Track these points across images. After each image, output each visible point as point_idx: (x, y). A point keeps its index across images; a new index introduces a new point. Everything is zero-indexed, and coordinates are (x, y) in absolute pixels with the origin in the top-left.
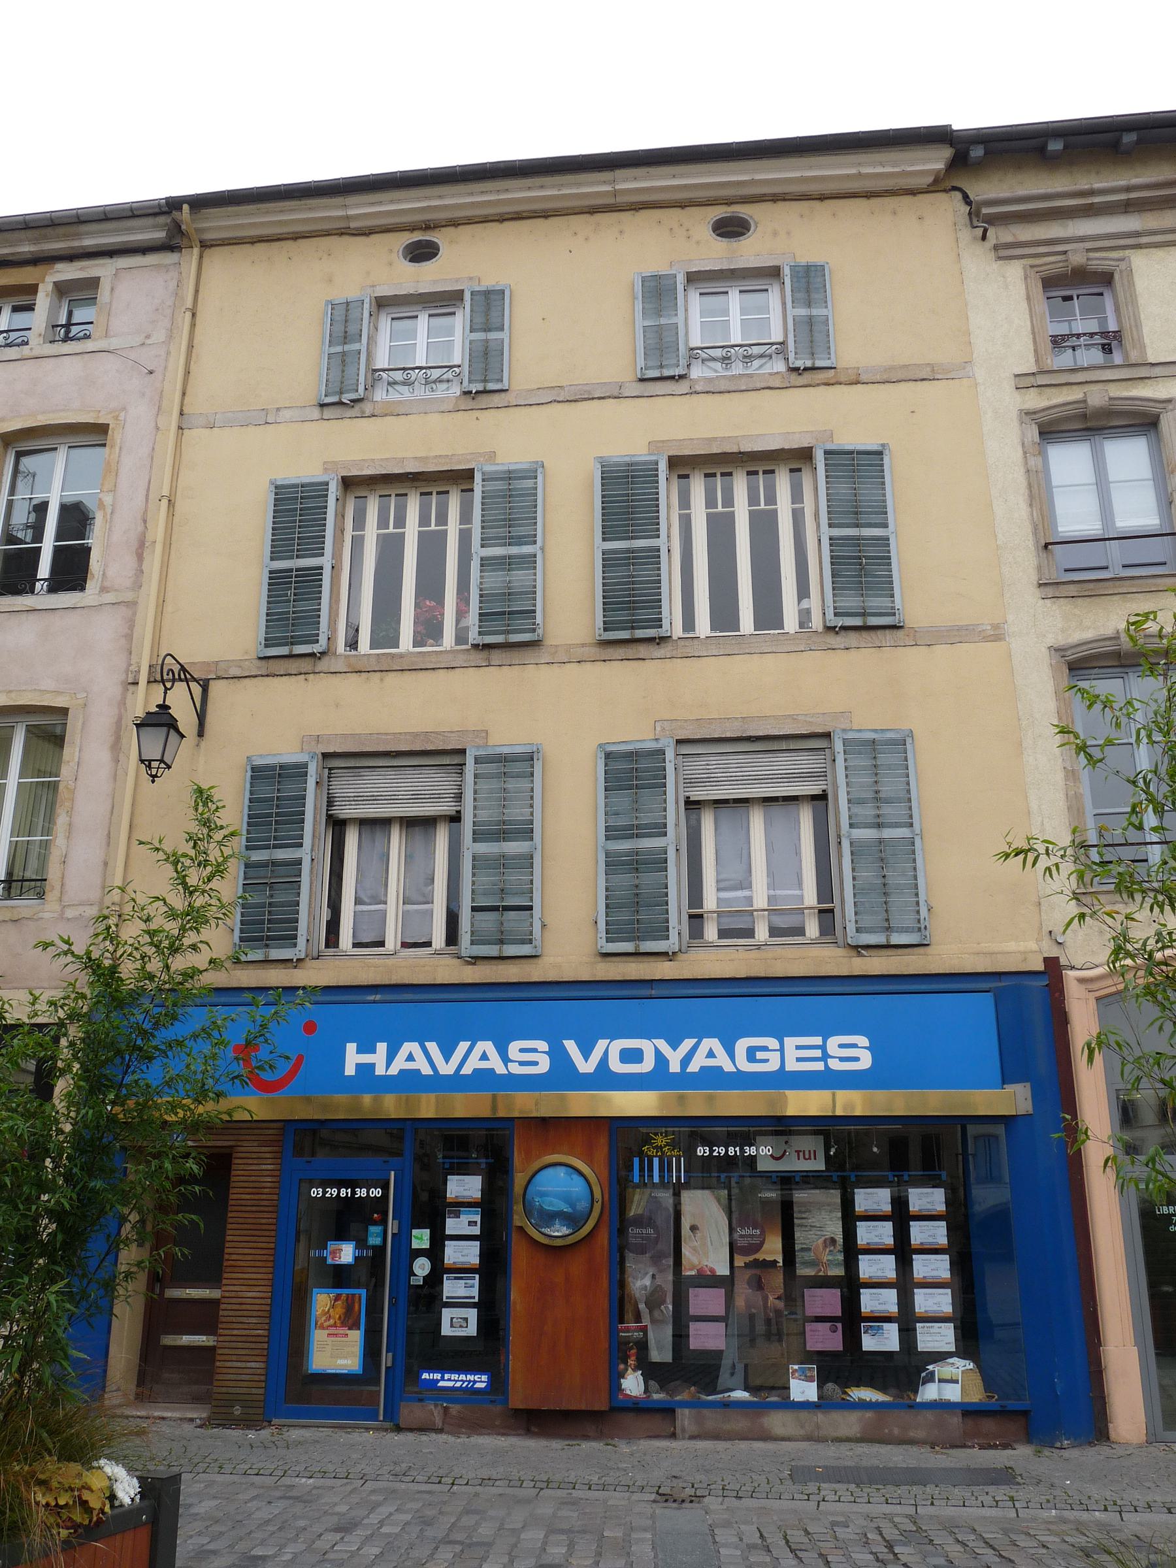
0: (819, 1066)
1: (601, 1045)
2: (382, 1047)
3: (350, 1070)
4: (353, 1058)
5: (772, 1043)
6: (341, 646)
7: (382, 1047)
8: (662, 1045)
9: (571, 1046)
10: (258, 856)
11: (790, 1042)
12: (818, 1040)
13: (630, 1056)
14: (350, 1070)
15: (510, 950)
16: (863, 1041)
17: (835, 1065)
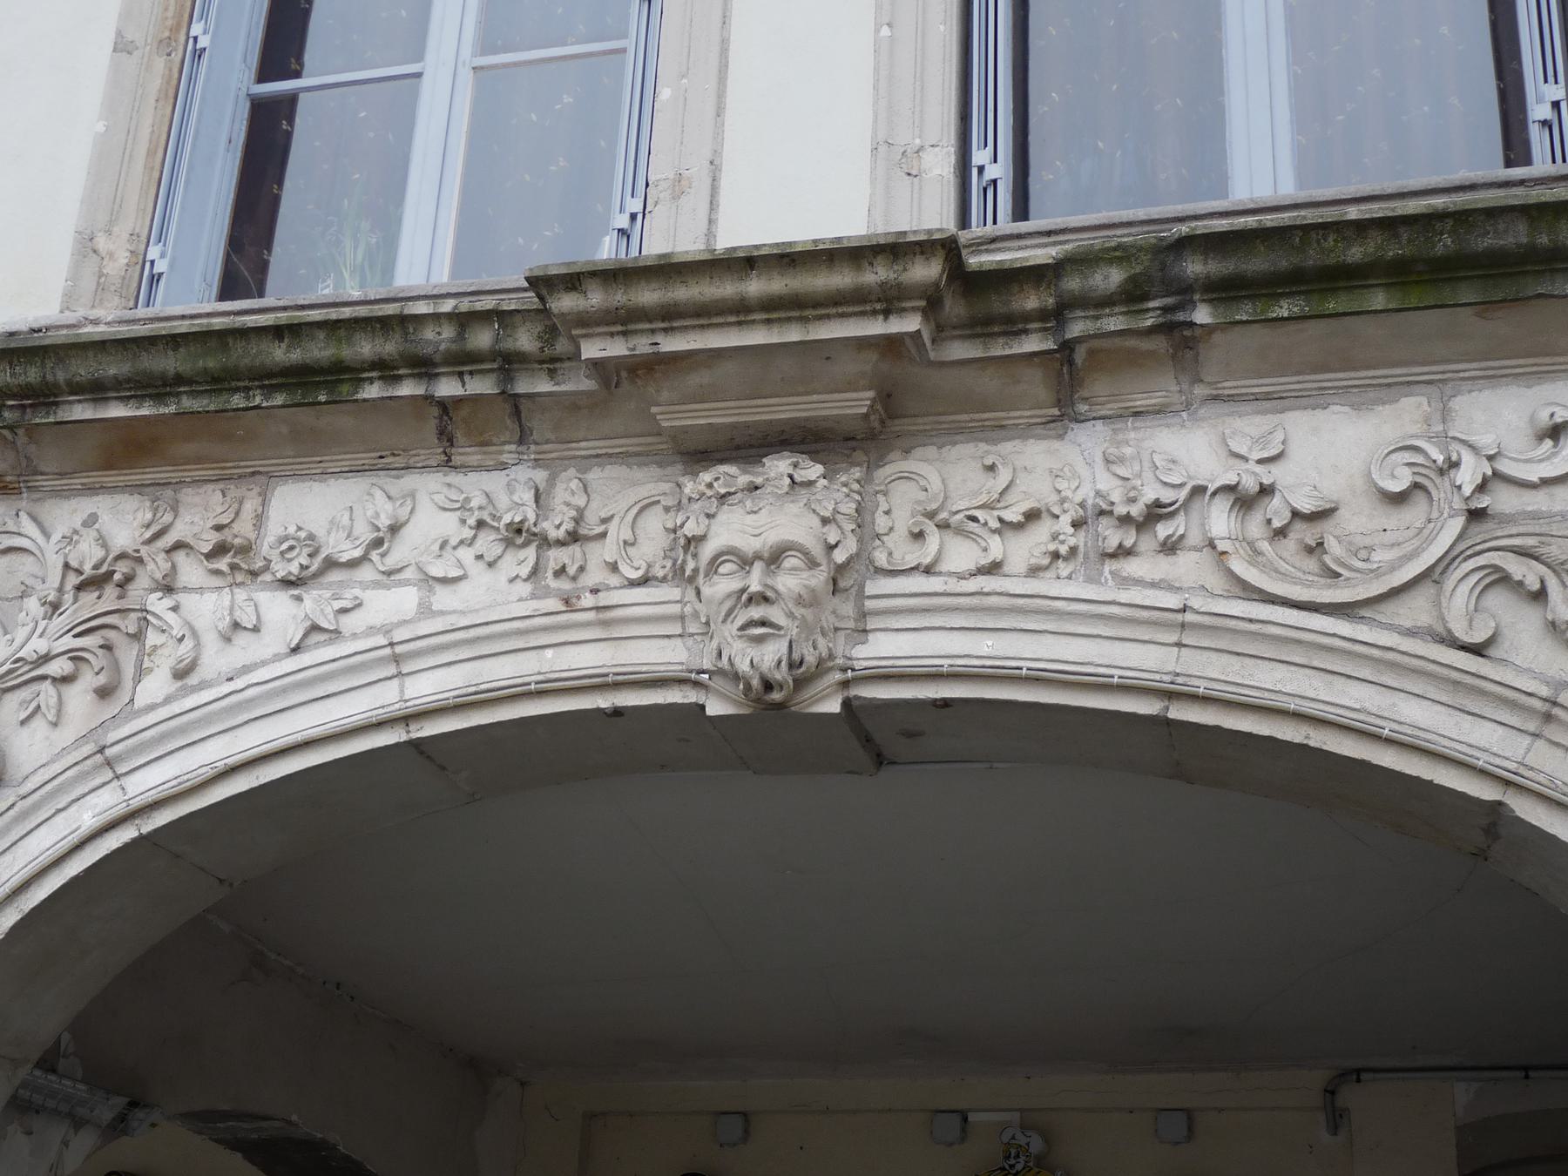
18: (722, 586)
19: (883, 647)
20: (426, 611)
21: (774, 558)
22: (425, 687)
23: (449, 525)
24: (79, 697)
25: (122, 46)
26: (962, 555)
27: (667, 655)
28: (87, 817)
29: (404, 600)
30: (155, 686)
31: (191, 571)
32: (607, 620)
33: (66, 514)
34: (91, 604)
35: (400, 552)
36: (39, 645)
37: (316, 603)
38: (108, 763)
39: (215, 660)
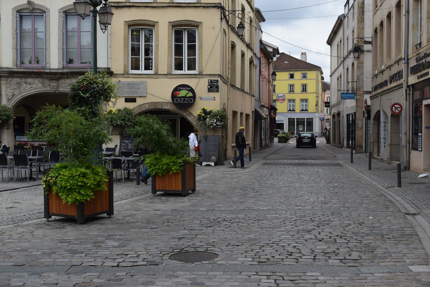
18: (52, 87)
19: (60, 89)
20: (37, 87)
21: (54, 86)
22: (37, 90)
23: (37, 82)
24: (18, 90)
25: (13, 48)
26: (63, 85)
27: (49, 89)
28: (20, 96)
29: (35, 86)
30: (22, 90)
31: (23, 83)
32: (46, 88)
33: (15, 79)
34: (18, 85)
35: (35, 83)
36: (15, 87)
37: (31, 86)
38: (20, 94)
39: (26, 88)
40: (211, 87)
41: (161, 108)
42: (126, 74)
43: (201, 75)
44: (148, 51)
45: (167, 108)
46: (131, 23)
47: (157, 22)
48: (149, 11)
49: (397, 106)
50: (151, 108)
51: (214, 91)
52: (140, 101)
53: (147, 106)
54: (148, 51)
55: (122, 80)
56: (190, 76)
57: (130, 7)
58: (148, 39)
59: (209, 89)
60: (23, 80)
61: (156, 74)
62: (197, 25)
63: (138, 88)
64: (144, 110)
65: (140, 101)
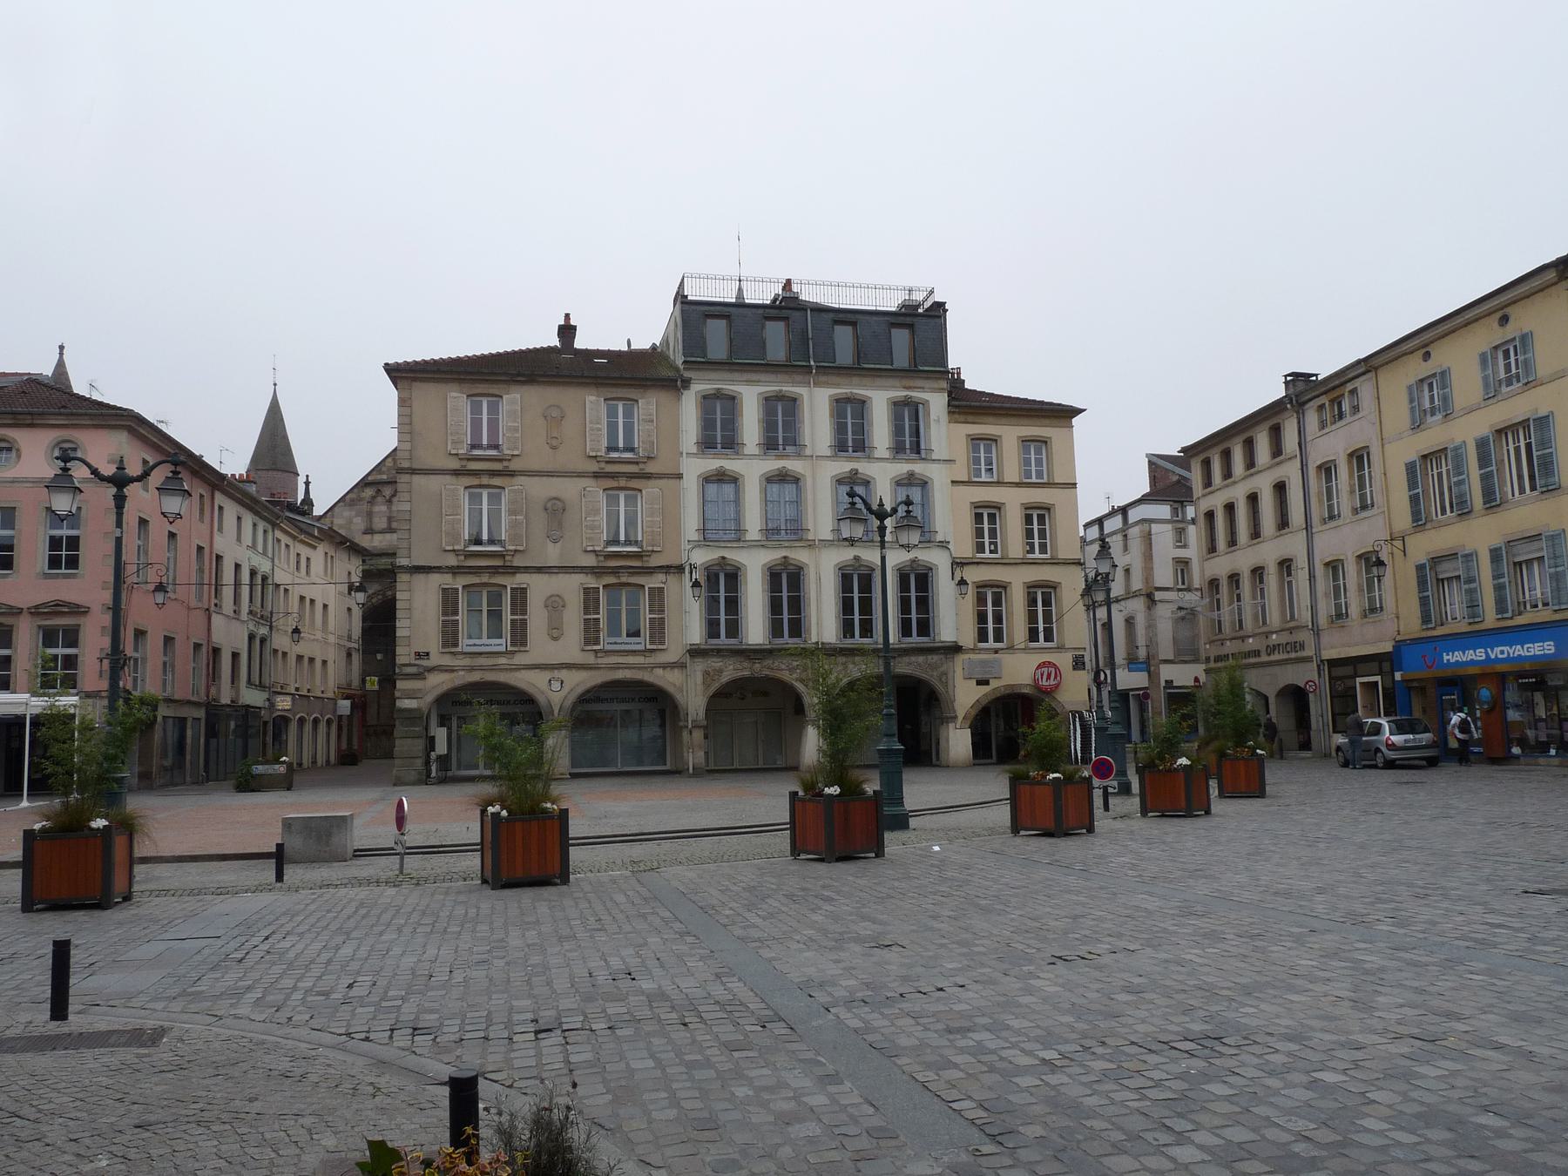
0: (1542, 652)
1: (1495, 649)
2: (1451, 654)
3: (1445, 661)
4: (1446, 657)
5: (1531, 645)
6: (1434, 518)
7: (1451, 654)
8: (1508, 648)
9: (1489, 649)
10: (1421, 595)
11: (1536, 644)
12: (1541, 644)
13: (1502, 652)
14: (1445, 661)
15: (1476, 620)
16: (1552, 643)
17: (1546, 652)
19: (896, 670)
40: (1076, 664)
41: (1019, 691)
42: (973, 650)
43: (1061, 648)
44: (998, 619)
45: (1026, 691)
46: (981, 584)
47: (1010, 583)
48: (999, 569)
49: (1310, 683)
50: (1007, 692)
51: (1080, 669)
52: (994, 684)
53: (1002, 689)
54: (998, 619)
55: (972, 656)
56: (1051, 651)
57: (978, 563)
58: (997, 602)
59: (1073, 666)
60: (850, 659)
61: (1011, 648)
62: (1054, 586)
63: (993, 667)
64: (999, 695)
65: (994, 684)
